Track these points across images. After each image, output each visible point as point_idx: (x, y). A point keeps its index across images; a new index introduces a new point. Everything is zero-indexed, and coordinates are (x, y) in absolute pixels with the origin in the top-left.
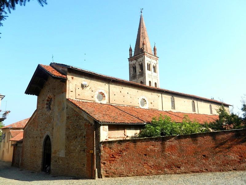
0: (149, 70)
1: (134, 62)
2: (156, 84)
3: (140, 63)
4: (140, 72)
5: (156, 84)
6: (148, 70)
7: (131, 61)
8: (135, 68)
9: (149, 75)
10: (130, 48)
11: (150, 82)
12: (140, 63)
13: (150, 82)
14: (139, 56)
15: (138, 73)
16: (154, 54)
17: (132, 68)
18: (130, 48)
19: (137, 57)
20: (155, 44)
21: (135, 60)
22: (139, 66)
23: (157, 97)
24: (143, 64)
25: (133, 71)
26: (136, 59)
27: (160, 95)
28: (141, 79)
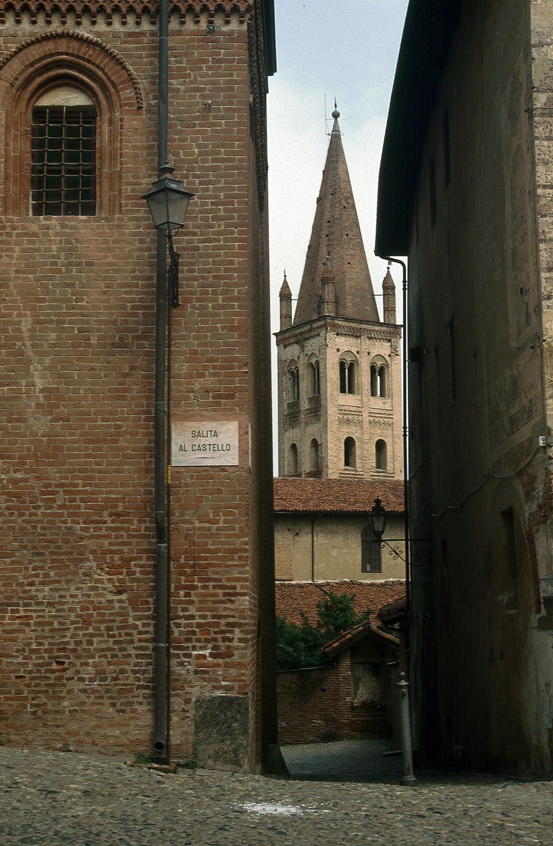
0: (351, 391)
2: (381, 446)
3: (313, 361)
4: (310, 400)
5: (381, 446)
6: (343, 390)
7: (285, 347)
11: (349, 443)
12: (313, 361)
13: (349, 443)
15: (305, 405)
16: (386, 310)
17: (289, 376)
19: (301, 333)
21: (296, 343)
22: (311, 370)
24: (321, 365)
25: (290, 389)
26: (301, 341)
28: (313, 430)
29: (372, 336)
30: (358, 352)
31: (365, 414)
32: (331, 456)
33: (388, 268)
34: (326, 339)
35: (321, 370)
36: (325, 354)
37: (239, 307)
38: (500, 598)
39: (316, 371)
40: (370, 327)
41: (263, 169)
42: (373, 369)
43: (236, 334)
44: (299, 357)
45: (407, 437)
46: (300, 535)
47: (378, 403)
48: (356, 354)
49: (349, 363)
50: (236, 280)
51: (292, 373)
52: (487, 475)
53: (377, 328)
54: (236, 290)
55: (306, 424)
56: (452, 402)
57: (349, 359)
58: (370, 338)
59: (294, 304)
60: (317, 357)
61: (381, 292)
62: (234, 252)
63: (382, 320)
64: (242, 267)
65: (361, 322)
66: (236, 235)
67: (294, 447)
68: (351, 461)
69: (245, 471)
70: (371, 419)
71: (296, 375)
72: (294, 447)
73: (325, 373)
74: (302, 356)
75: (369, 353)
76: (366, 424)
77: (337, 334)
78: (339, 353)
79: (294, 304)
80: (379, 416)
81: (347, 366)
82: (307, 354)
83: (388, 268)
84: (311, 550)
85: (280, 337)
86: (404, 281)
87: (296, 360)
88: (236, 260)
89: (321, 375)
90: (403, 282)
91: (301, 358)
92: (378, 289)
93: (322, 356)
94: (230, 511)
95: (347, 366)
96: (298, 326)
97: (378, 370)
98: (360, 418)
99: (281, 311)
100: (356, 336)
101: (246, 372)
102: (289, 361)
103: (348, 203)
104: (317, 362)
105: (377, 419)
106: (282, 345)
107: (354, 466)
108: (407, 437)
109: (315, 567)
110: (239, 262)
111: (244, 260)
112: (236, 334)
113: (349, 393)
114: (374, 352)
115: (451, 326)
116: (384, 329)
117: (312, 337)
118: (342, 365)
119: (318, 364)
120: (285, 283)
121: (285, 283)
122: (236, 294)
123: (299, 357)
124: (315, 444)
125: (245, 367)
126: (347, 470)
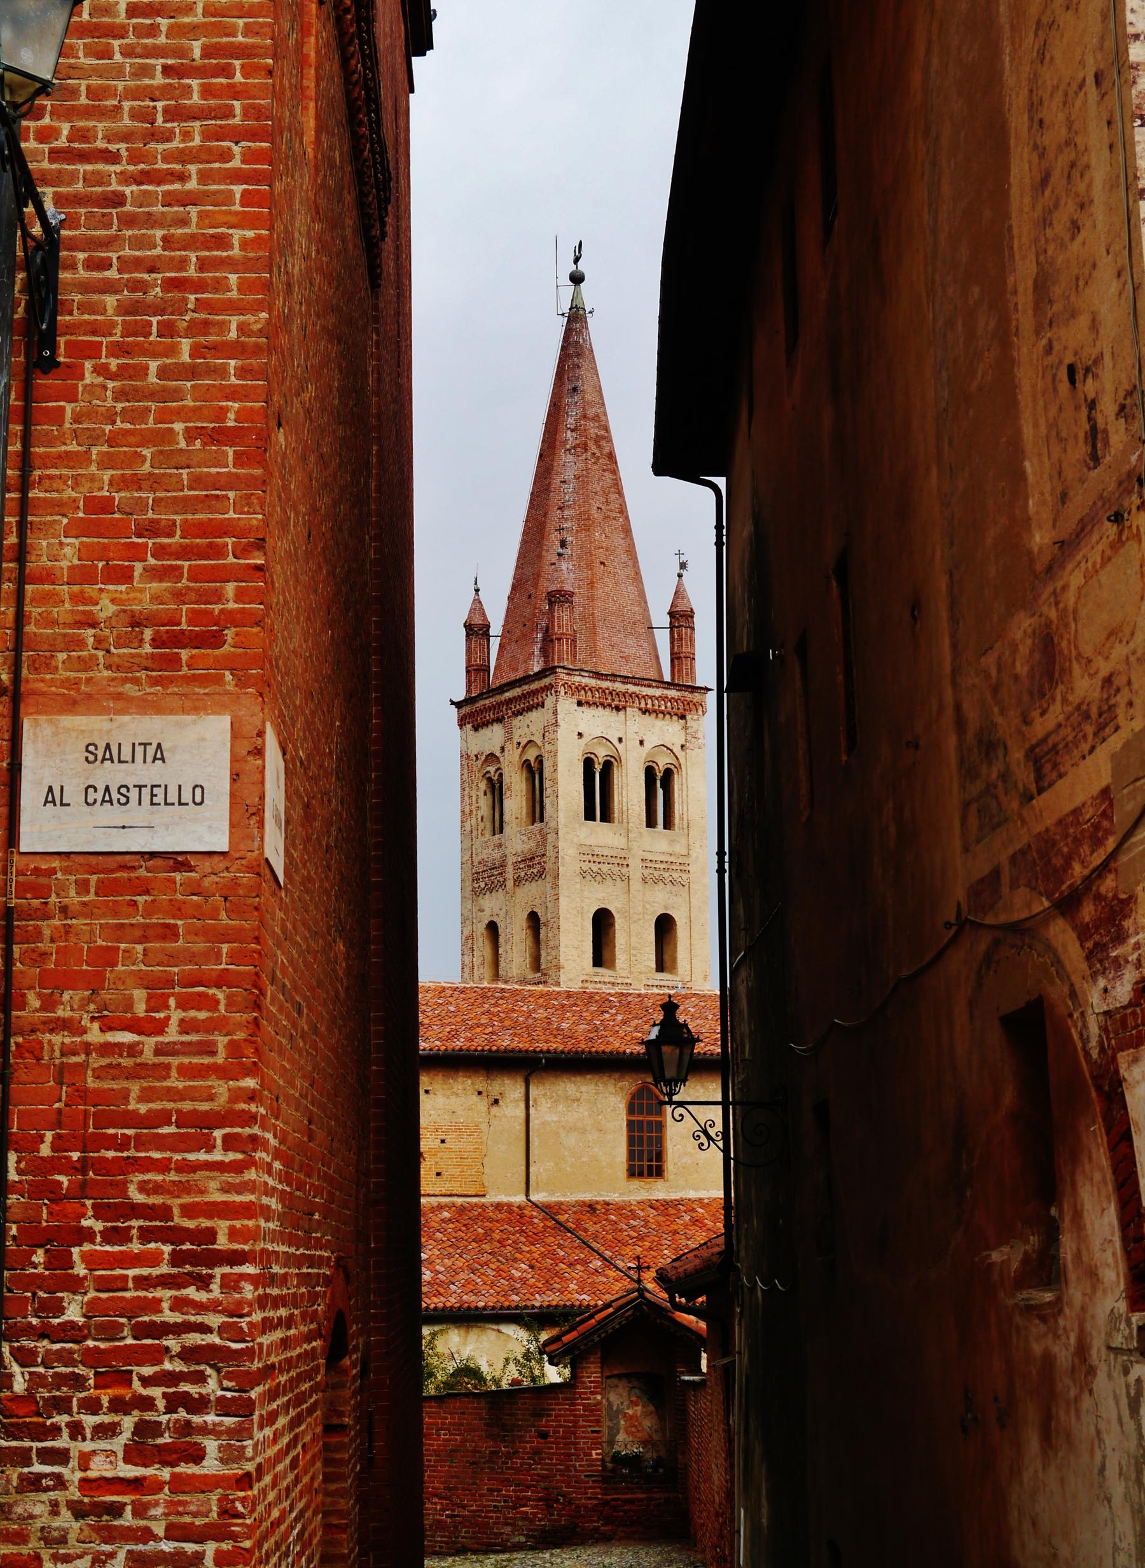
0: (606, 817)
1: (492, 738)
2: (665, 926)
3: (531, 755)
5: (665, 926)
6: (589, 815)
8: (496, 789)
9: (591, 855)
10: (477, 607)
11: (603, 922)
13: (603, 922)
14: (524, 696)
16: (675, 657)
18: (477, 607)
20: (683, 566)
23: (482, 1104)
27: (511, 1089)
28: (529, 895)
29: (650, 706)
30: (620, 740)
31: (635, 864)
32: (567, 946)
33: (680, 576)
34: (555, 713)
35: (547, 773)
36: (554, 742)
37: (242, 372)
38: (996, 1256)
39: (537, 776)
40: (646, 691)
41: (372, 150)
42: (650, 772)
43: (230, 451)
44: (503, 749)
45: (727, 875)
46: (501, 1103)
47: (658, 842)
48: (616, 742)
49: (602, 760)
50: (234, 294)
51: (490, 780)
52: (953, 921)
53: (658, 692)
54: (234, 321)
55: (518, 882)
56: (844, 758)
57: (602, 753)
58: (645, 711)
59: (495, 644)
60: (540, 748)
61: (666, 621)
62: (230, 213)
63: (667, 678)
64: (252, 255)
65: (625, 679)
66: (236, 163)
67: (492, 927)
68: (606, 955)
69: (249, 868)
70: (647, 872)
71: (497, 786)
72: (492, 927)
73: (555, 781)
74: (508, 746)
75: (641, 743)
76: (636, 884)
77: (580, 704)
79: (495, 644)
80: (662, 866)
81: (598, 768)
82: (519, 744)
83: (680, 576)
84: (523, 1135)
85: (466, 709)
86: (719, 527)
87: (498, 754)
88: (237, 234)
89: (547, 784)
90: (716, 527)
91: (506, 750)
92: (660, 618)
93: (548, 747)
94: (200, 994)
95: (598, 768)
96: (502, 689)
97: (659, 775)
98: (624, 870)
99: (468, 660)
100: (618, 709)
101: (259, 568)
102: (483, 758)
103: (599, 447)
104: (540, 760)
105: (656, 873)
106: (469, 726)
107: (611, 965)
108: (727, 875)
109: (532, 1169)
110: (245, 244)
111: (259, 237)
112: (230, 451)
113: (602, 820)
114: (651, 741)
115: (842, 570)
116: (672, 693)
117: (530, 709)
118: (588, 764)
119: (541, 763)
120: (477, 601)
121: (477, 601)
122: (233, 335)
123: (503, 749)
124: (534, 921)
125: (257, 553)
126: (596, 974)
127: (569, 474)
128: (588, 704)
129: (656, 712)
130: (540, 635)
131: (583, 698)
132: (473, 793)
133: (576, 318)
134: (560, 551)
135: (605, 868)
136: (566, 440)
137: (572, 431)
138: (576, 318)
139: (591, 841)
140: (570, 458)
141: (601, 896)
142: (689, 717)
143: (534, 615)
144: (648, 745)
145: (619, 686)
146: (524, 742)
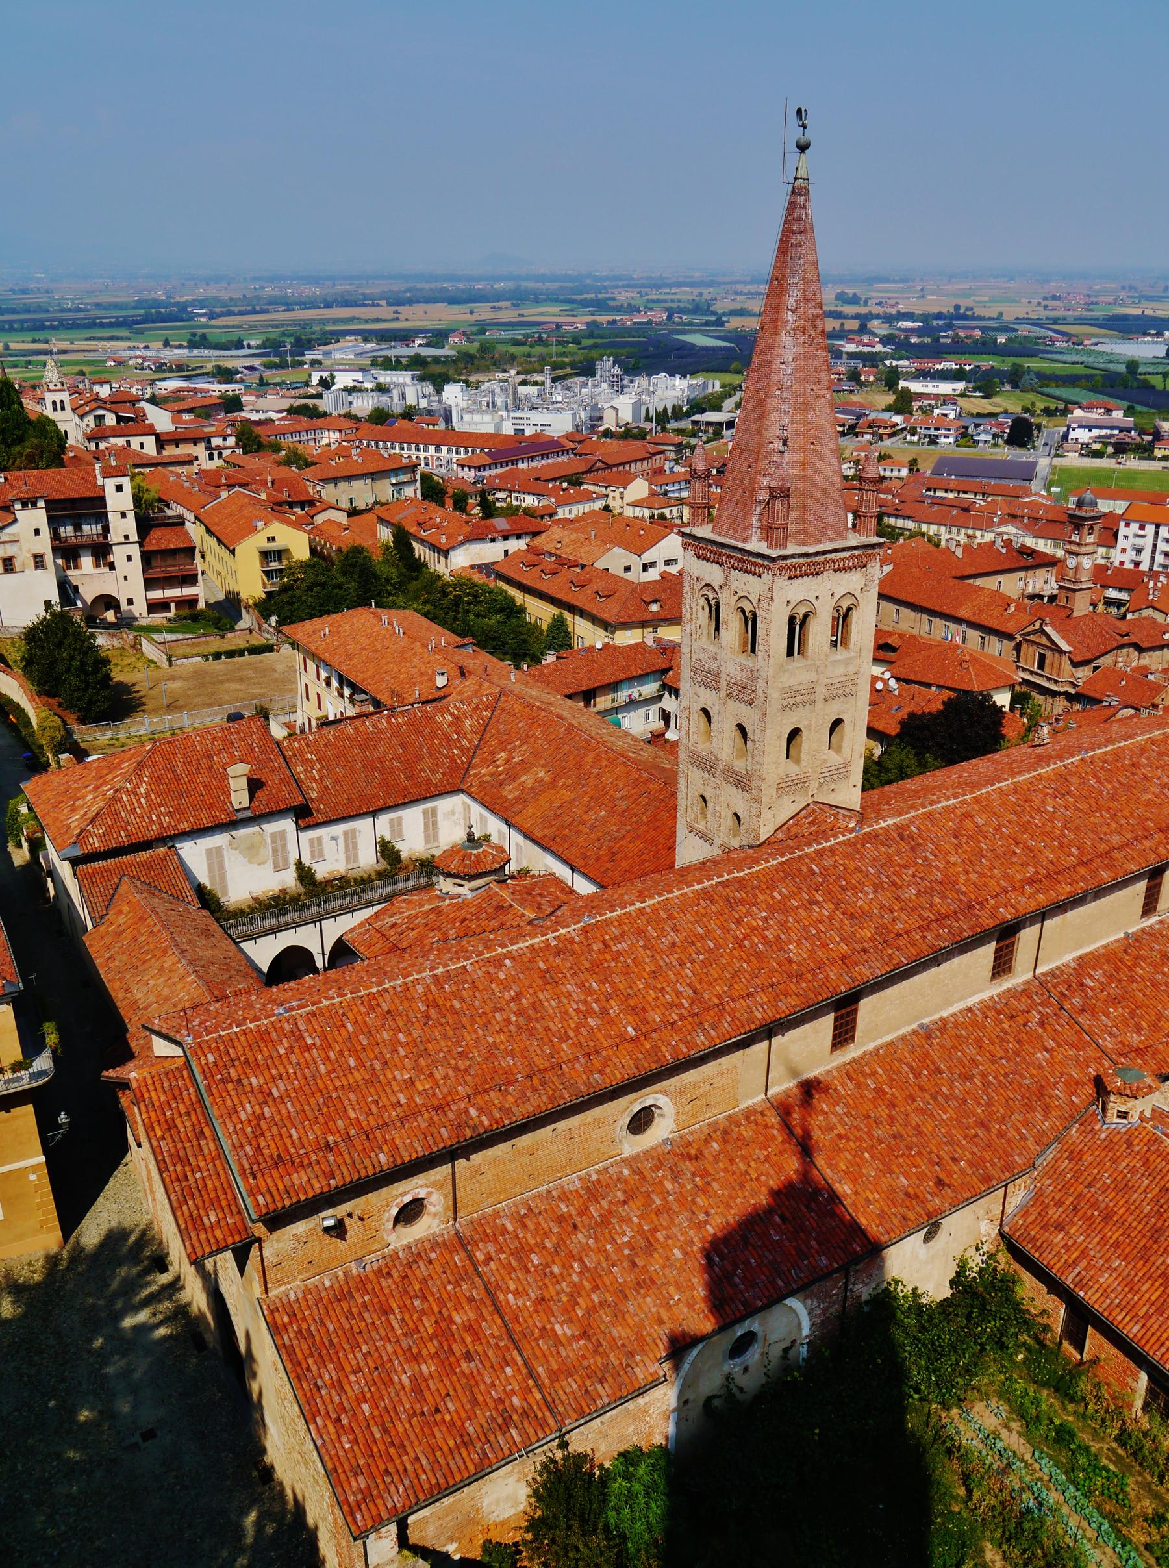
77: (790, 578)
78: (791, 606)
81: (798, 622)
95: (798, 622)
100: (817, 574)
103: (815, 327)
117: (748, 572)
127: (788, 356)
128: (796, 577)
129: (845, 569)
130: (758, 509)
131: (793, 574)
132: (694, 606)
133: (799, 191)
134: (782, 448)
135: (798, 699)
136: (787, 322)
137: (793, 312)
138: (799, 191)
139: (791, 682)
140: (790, 341)
141: (793, 720)
142: (869, 566)
143: (753, 488)
144: (837, 596)
145: (821, 558)
146: (741, 594)
